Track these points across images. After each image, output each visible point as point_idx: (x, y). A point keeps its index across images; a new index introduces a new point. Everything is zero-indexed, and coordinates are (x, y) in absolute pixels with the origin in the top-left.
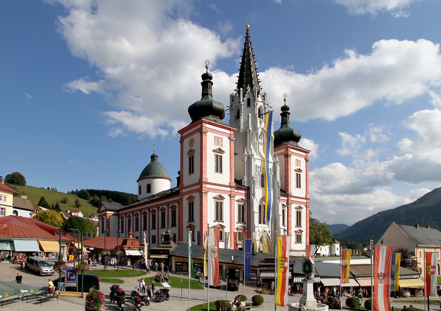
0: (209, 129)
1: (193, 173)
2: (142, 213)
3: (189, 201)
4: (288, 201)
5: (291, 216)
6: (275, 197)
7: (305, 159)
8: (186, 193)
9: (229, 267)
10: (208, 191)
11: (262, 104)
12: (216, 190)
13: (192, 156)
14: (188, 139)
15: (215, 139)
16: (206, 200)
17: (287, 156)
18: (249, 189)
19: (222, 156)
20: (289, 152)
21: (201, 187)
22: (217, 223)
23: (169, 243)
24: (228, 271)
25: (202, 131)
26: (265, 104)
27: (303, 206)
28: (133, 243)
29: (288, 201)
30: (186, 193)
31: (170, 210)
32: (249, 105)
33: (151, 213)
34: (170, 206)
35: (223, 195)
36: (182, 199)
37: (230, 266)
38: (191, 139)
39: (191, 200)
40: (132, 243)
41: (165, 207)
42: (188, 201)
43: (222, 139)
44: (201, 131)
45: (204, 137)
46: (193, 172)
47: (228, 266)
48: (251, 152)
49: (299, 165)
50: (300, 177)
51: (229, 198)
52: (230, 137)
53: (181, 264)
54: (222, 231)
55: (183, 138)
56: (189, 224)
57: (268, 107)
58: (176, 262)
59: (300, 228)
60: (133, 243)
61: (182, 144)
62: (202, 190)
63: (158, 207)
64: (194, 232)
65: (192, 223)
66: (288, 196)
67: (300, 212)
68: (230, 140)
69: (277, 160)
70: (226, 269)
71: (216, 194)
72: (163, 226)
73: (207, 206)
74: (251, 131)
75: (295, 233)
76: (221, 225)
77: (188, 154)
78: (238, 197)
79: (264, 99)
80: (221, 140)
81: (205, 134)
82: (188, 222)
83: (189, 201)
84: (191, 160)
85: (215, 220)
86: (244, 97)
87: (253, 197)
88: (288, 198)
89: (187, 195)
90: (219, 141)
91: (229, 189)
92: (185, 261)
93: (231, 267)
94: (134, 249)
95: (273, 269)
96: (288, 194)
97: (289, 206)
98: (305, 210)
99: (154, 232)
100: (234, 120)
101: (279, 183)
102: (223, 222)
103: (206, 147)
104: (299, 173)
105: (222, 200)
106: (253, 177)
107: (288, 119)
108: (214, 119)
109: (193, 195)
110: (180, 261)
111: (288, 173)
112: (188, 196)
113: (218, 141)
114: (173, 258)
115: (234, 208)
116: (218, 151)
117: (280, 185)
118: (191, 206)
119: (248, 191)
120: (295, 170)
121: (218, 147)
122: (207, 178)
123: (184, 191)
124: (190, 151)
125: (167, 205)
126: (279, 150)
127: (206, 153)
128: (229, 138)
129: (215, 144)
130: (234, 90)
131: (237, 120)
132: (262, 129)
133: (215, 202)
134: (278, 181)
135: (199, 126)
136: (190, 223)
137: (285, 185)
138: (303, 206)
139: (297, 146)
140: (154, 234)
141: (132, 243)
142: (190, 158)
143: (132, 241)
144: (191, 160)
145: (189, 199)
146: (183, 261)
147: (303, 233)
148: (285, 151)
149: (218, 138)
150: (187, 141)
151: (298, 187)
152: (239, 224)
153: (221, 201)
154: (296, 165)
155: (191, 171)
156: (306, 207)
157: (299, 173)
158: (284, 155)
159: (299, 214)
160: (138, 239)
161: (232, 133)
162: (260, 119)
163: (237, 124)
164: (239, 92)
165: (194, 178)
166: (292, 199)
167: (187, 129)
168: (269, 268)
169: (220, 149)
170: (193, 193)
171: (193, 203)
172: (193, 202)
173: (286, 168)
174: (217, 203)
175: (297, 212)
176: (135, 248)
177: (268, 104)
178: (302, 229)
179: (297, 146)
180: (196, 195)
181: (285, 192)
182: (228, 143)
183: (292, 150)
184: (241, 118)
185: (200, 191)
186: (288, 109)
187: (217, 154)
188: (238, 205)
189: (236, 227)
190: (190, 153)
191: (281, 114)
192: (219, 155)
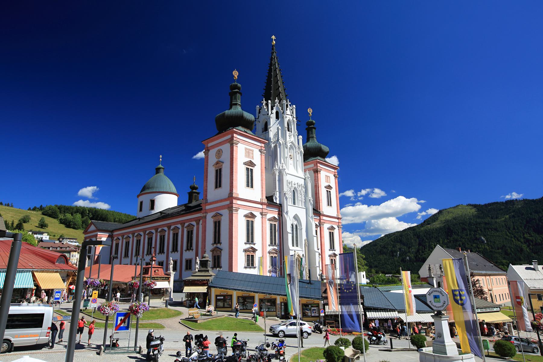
0: (240, 140)
2: (147, 233)
4: (320, 220)
5: (324, 237)
6: (307, 214)
8: (211, 210)
10: (239, 207)
13: (220, 168)
14: (216, 149)
15: (245, 150)
17: (316, 171)
18: (282, 207)
19: (252, 169)
20: (319, 168)
21: (232, 203)
22: (248, 246)
23: (208, 271)
24: (283, 305)
28: (157, 271)
29: (320, 220)
30: (211, 210)
35: (254, 213)
37: (286, 299)
40: (155, 271)
41: (179, 226)
42: (213, 219)
43: (253, 151)
45: (235, 148)
46: (220, 186)
47: (283, 299)
48: (282, 167)
49: (329, 181)
50: (330, 194)
51: (260, 216)
53: (222, 298)
54: (253, 255)
56: (213, 247)
58: (217, 296)
59: (334, 252)
60: (157, 271)
61: (207, 155)
62: (232, 207)
63: (168, 226)
64: (221, 256)
65: (219, 245)
67: (333, 233)
68: (261, 153)
70: (281, 303)
71: (247, 212)
72: (175, 249)
73: (237, 225)
75: (329, 257)
76: (252, 248)
78: (270, 216)
80: (251, 152)
81: (236, 145)
83: (215, 219)
89: (212, 212)
91: (260, 206)
92: (228, 294)
94: (158, 280)
96: (320, 212)
97: (321, 226)
98: (338, 231)
100: (261, 132)
102: (254, 244)
103: (236, 159)
106: (285, 193)
110: (222, 293)
111: (318, 189)
112: (213, 213)
113: (248, 152)
114: (213, 290)
115: (266, 227)
117: (312, 202)
118: (217, 225)
120: (326, 187)
121: (249, 159)
122: (238, 193)
123: (208, 207)
124: (217, 163)
125: (181, 224)
126: (307, 165)
127: (237, 165)
129: (246, 156)
133: (246, 221)
134: (310, 198)
136: (215, 245)
137: (316, 203)
139: (326, 162)
141: (155, 271)
142: (217, 171)
143: (155, 269)
145: (214, 216)
146: (226, 293)
147: (337, 256)
148: (315, 166)
151: (329, 205)
152: (272, 247)
154: (326, 182)
156: (338, 227)
157: (329, 190)
158: (313, 170)
159: (331, 235)
160: (162, 265)
161: (263, 145)
162: (289, 132)
165: (223, 192)
166: (324, 218)
170: (220, 210)
171: (219, 222)
172: (219, 220)
173: (316, 184)
174: (248, 221)
175: (330, 232)
179: (326, 162)
180: (225, 212)
181: (317, 211)
184: (270, 130)
185: (230, 208)
187: (248, 167)
189: (268, 250)
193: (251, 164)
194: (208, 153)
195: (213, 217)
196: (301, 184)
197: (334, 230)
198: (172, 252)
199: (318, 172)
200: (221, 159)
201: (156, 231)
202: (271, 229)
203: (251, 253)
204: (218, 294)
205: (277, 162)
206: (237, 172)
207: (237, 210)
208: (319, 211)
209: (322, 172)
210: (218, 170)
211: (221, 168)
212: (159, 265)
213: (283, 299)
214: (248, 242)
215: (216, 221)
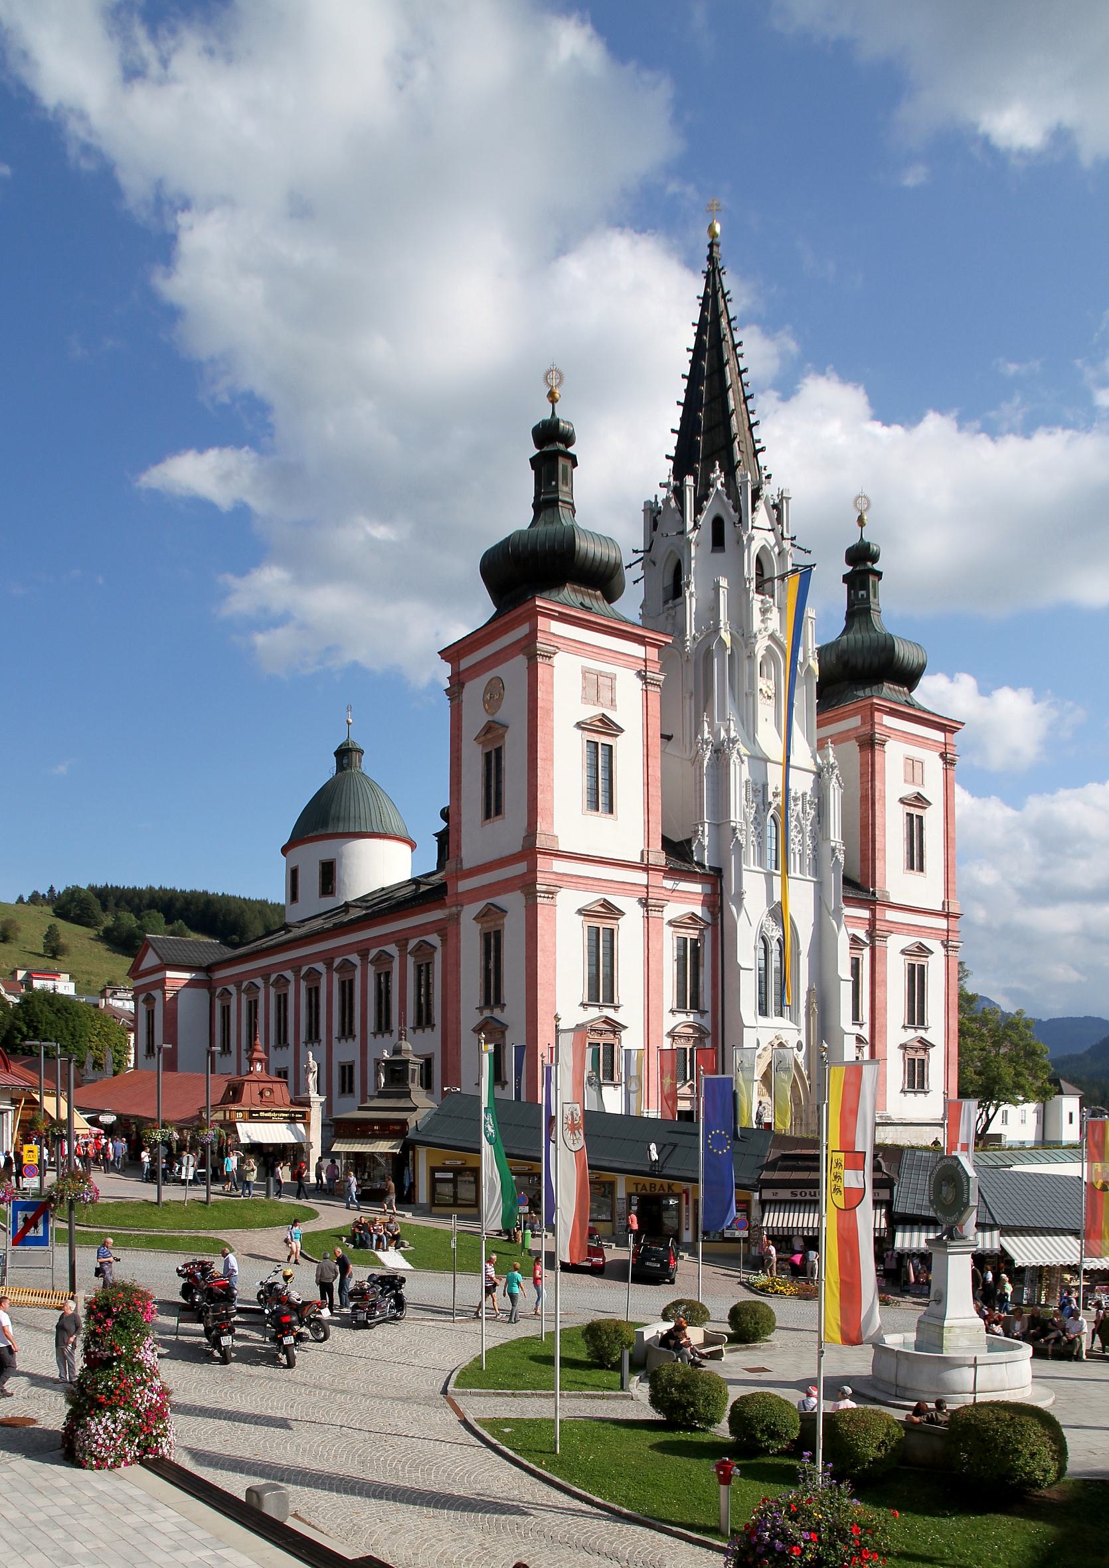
0: (562, 641)
1: (500, 816)
3: (485, 925)
4: (872, 922)
5: (885, 982)
7: (943, 756)
8: (475, 895)
9: (640, 1187)
10: (559, 883)
11: (771, 538)
12: (591, 882)
13: (497, 746)
15: (584, 678)
16: (552, 920)
17: (869, 744)
19: (611, 747)
21: (533, 870)
22: (594, 1013)
23: (407, 1095)
25: (536, 649)
26: (783, 539)
27: (934, 945)
28: (268, 1094)
29: (872, 922)
30: (475, 895)
31: (410, 961)
32: (718, 541)
33: (336, 976)
34: (410, 947)
36: (456, 918)
37: (644, 1185)
38: (492, 680)
39: (492, 924)
40: (261, 1094)
41: (392, 949)
42: (479, 926)
43: (613, 678)
44: (529, 650)
45: (541, 670)
46: (499, 811)
48: (728, 731)
49: (918, 779)
51: (640, 911)
52: (645, 672)
53: (450, 1175)
54: (613, 1045)
55: (461, 676)
56: (483, 1017)
57: (793, 550)
58: (433, 1170)
59: (921, 1033)
60: (268, 1094)
62: (534, 882)
64: (504, 1047)
65: (497, 1013)
66: (874, 902)
67: (922, 968)
68: (646, 683)
69: (832, 760)
70: (630, 1195)
71: (588, 898)
72: (384, 1026)
74: (729, 645)
76: (607, 1021)
77: (482, 739)
78: (674, 910)
79: (779, 520)
80: (608, 682)
81: (547, 661)
82: (480, 1009)
84: (493, 764)
85: (586, 1001)
86: (698, 510)
87: (734, 909)
88: (873, 912)
90: (601, 687)
93: (648, 1188)
95: (815, 1196)
96: (874, 894)
98: (943, 960)
99: (347, 1052)
100: (662, 603)
101: (840, 850)
102: (616, 1008)
103: (549, 711)
104: (916, 812)
105: (615, 922)
106: (734, 829)
107: (875, 597)
108: (580, 599)
109: (501, 900)
110: (447, 1162)
112: (477, 907)
115: (662, 950)
116: (598, 726)
117: (841, 858)
118: (492, 944)
119: (714, 886)
120: (902, 801)
122: (556, 833)
123: (464, 885)
125: (397, 942)
126: (839, 720)
128: (642, 675)
129: (585, 699)
130: (660, 484)
131: (670, 604)
132: (772, 637)
133: (586, 929)
134: (833, 844)
135: (523, 630)
136: (487, 1013)
137: (862, 861)
138: (934, 945)
139: (911, 705)
140: (346, 1059)
141: (261, 1094)
142: (488, 756)
143: (262, 1085)
144: (493, 764)
147: (931, 1051)
148: (863, 723)
149: (599, 674)
150: (474, 690)
151: (912, 868)
152: (682, 1018)
153: (609, 923)
154: (905, 781)
155: (493, 806)
156: (946, 947)
157: (916, 812)
159: (916, 979)
160: (286, 1077)
161: (653, 653)
162: (761, 597)
163: (669, 618)
164: (679, 493)
166: (891, 915)
167: (477, 640)
168: (799, 1191)
169: (605, 721)
170: (498, 894)
171: (498, 935)
173: (867, 790)
174: (594, 933)
175: (912, 967)
176: (275, 1115)
177: (793, 539)
178: (928, 1036)
180: (512, 901)
182: (639, 695)
183: (888, 721)
184: (687, 595)
185: (528, 885)
186: (874, 558)
187: (596, 738)
188: (675, 939)
189: (667, 1029)
190: (489, 736)
191: (846, 578)
192: (602, 744)
193: (607, 726)
194: (460, 693)
195: (480, 917)
196: (804, 795)
197: (927, 957)
198: (375, 1034)
199: (877, 747)
200: (500, 716)
201: (329, 966)
202: (681, 961)
203: (604, 1036)
204: (438, 1164)
205: (711, 716)
206: (552, 760)
207: (551, 894)
208: (871, 889)
209: (891, 746)
210: (491, 752)
211: (501, 748)
212: (279, 1076)
213: (637, 1184)
214: (593, 998)
215: (487, 931)
